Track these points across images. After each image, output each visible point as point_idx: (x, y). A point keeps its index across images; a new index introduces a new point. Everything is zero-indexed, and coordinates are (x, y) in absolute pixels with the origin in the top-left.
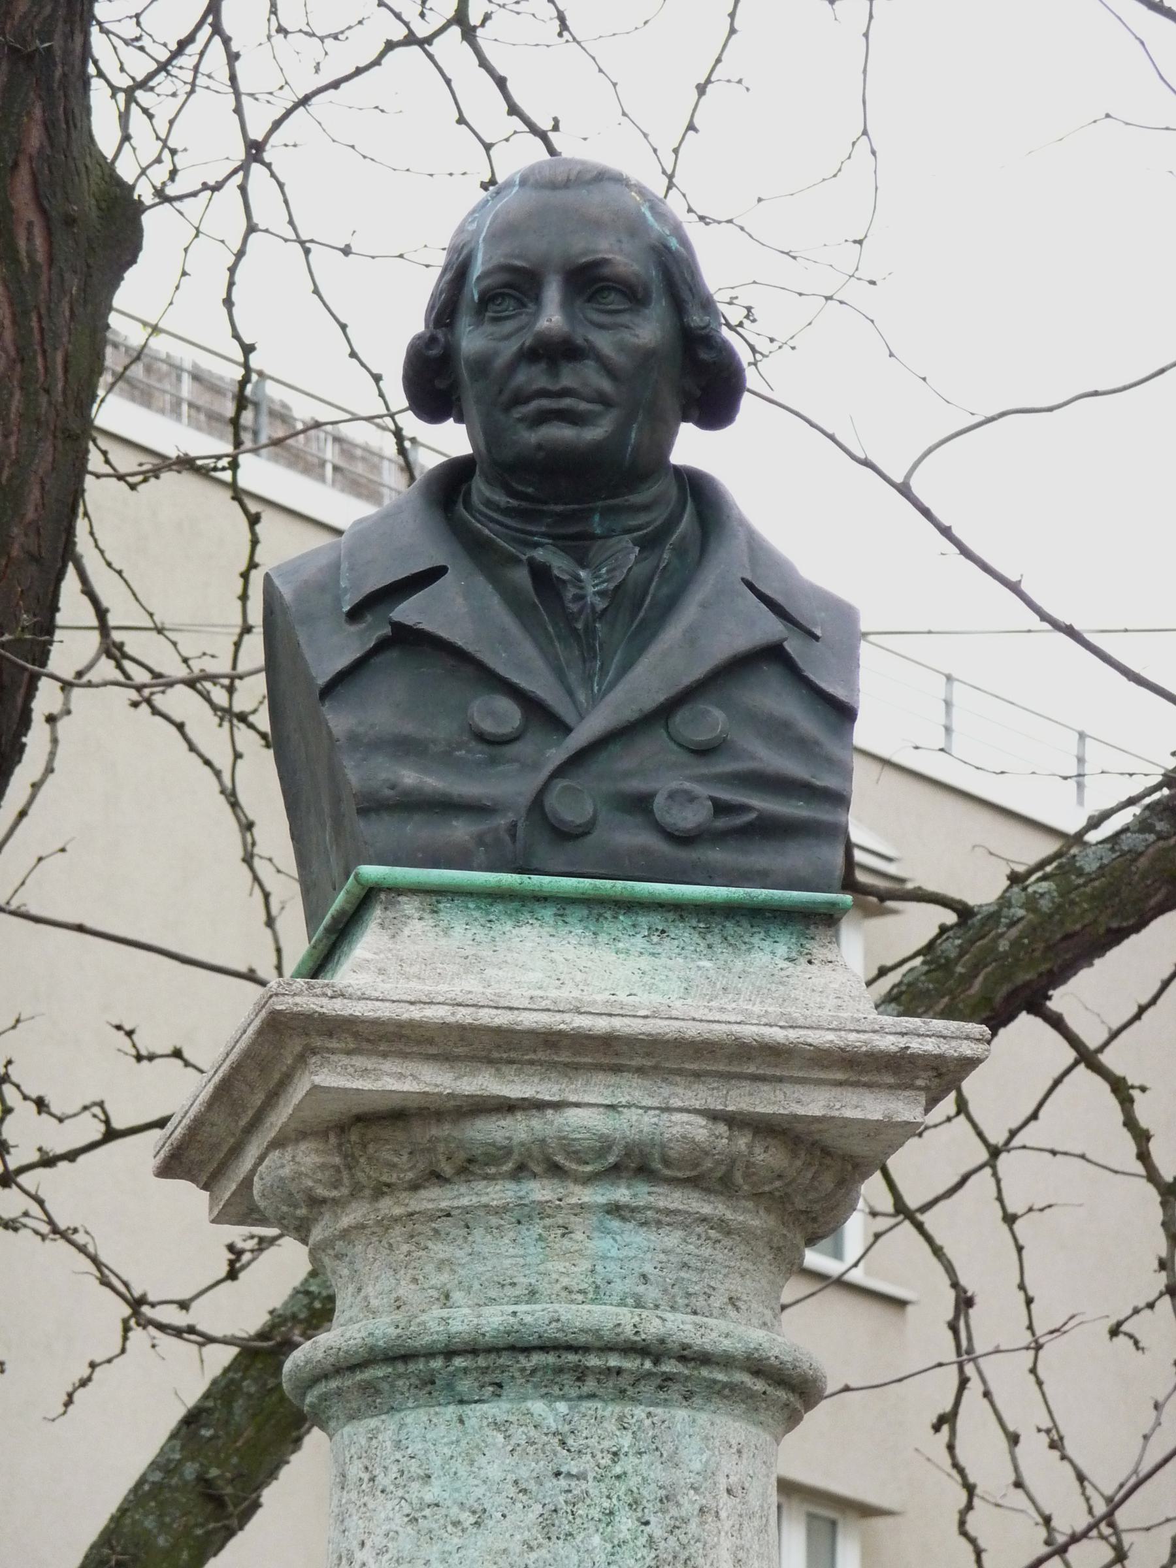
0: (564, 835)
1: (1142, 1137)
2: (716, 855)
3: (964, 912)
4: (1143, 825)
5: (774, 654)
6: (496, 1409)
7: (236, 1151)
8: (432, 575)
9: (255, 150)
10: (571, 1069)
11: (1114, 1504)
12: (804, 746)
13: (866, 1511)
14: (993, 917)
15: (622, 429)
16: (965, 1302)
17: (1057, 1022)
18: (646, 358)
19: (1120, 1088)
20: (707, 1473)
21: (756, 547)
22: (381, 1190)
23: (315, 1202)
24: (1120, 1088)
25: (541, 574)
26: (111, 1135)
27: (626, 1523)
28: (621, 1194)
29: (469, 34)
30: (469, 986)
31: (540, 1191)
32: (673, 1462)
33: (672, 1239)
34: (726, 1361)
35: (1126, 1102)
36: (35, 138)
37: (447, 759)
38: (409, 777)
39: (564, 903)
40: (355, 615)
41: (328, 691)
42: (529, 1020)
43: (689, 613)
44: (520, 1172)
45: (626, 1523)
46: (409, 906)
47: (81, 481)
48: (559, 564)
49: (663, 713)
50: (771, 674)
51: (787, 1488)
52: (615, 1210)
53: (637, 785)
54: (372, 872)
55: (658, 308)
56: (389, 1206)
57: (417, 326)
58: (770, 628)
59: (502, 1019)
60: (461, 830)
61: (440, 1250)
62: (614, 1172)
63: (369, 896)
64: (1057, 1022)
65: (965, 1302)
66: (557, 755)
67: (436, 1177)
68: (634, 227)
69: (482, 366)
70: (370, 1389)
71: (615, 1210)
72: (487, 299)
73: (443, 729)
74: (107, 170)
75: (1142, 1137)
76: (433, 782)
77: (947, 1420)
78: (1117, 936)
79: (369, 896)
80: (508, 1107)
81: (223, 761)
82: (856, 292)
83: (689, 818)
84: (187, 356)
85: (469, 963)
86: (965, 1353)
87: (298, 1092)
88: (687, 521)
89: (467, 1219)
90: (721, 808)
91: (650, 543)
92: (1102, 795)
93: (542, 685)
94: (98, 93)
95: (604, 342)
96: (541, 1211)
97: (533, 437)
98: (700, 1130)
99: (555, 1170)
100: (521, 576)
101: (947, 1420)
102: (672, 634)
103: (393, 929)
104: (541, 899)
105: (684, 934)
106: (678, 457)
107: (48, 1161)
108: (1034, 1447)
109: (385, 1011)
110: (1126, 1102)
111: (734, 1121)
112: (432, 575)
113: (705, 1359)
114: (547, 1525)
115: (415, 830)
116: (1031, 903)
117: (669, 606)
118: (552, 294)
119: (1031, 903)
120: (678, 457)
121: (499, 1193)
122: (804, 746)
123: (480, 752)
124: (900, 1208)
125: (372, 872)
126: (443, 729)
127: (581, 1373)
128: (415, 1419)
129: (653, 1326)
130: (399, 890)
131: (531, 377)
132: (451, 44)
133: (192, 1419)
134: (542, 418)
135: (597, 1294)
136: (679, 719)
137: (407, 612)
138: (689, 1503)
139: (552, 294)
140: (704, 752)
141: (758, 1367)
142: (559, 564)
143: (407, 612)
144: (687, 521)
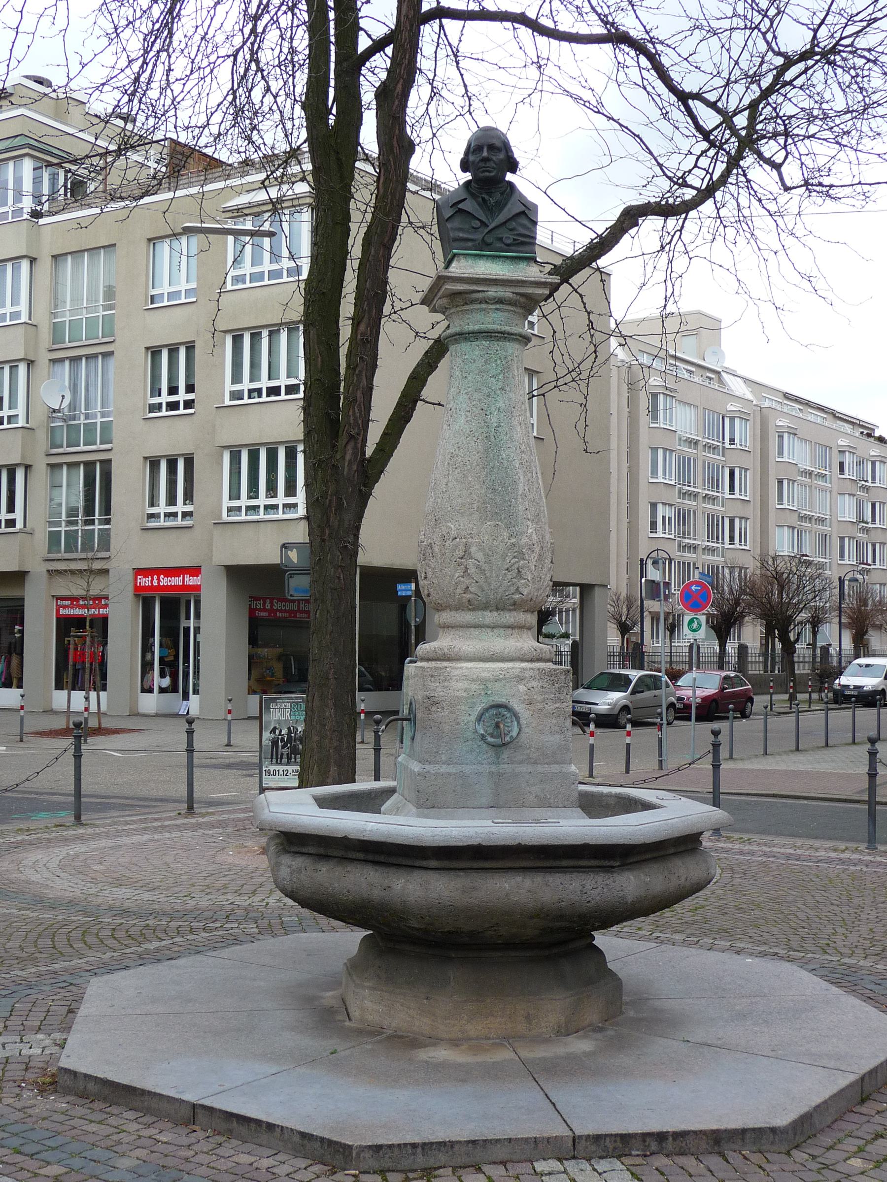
0: (488, 245)
1: (584, 304)
2: (513, 248)
3: (555, 266)
4: (585, 251)
5: (523, 213)
6: (476, 343)
7: (433, 300)
8: (465, 200)
9: (434, 135)
10: (489, 285)
11: (579, 365)
12: (528, 229)
13: (538, 372)
14: (560, 267)
15: (497, 173)
16: (555, 332)
17: (570, 285)
18: (501, 160)
19: (581, 296)
20: (512, 353)
21: (520, 194)
22: (457, 306)
23: (446, 308)
24: (581, 296)
25: (483, 199)
26: (412, 305)
27: (499, 362)
28: (498, 306)
29: (471, 114)
30: (472, 271)
31: (484, 306)
32: (507, 351)
33: (506, 314)
34: (516, 335)
35: (582, 298)
36: (397, 131)
37: (468, 232)
38: (461, 235)
39: (488, 256)
40: (452, 207)
41: (447, 220)
42: (482, 276)
43: (509, 206)
44: (481, 303)
45: (499, 362)
46: (461, 257)
47: (403, 197)
48: (486, 197)
49: (505, 222)
50: (523, 216)
51: (526, 369)
52: (497, 309)
53: (500, 236)
54: (455, 251)
55: (503, 152)
56: (458, 309)
57: (462, 156)
58: (523, 208)
59: (477, 276)
60: (470, 244)
61: (467, 316)
62: (496, 303)
63: (455, 255)
64: (570, 285)
65: (555, 332)
66: (486, 231)
67: (467, 304)
68: (499, 138)
69: (473, 162)
70: (456, 339)
71: (497, 309)
72: (474, 151)
73: (467, 226)
74: (410, 138)
75: (584, 304)
76: (465, 236)
77: (552, 352)
78: (581, 269)
79: (455, 255)
80: (479, 291)
81: (429, 242)
82: (536, 158)
83: (509, 242)
84: (423, 177)
85: (472, 267)
86: (555, 341)
87: (443, 289)
88: (508, 190)
89: (472, 311)
90: (514, 240)
91: (502, 194)
92: (578, 246)
93: (484, 219)
94: (408, 126)
95: (494, 158)
96: (484, 309)
97: (482, 175)
98: (511, 295)
99: (487, 302)
100: (480, 199)
101: (552, 352)
102: (506, 209)
103: (459, 261)
104: (484, 256)
105: (508, 261)
106: (507, 179)
107: (402, 309)
108: (566, 356)
109: (458, 275)
110: (582, 298)
111: (517, 294)
112: (465, 200)
113: (512, 334)
114: (485, 362)
115: (462, 244)
116: (566, 264)
117: (506, 204)
118: (485, 149)
119: (566, 264)
120: (507, 179)
121: (477, 306)
122: (528, 229)
123: (473, 230)
124: (544, 316)
125: (455, 251)
126: (467, 226)
127: (491, 337)
128: (463, 345)
129: (503, 329)
130: (460, 254)
131: (482, 164)
132: (468, 116)
133: (427, 352)
134: (484, 171)
135: (494, 323)
136: (507, 224)
137: (460, 206)
138: (509, 358)
139: (485, 149)
140: (511, 230)
141: (521, 336)
142: (486, 197)
143: (460, 206)
144: (508, 190)
